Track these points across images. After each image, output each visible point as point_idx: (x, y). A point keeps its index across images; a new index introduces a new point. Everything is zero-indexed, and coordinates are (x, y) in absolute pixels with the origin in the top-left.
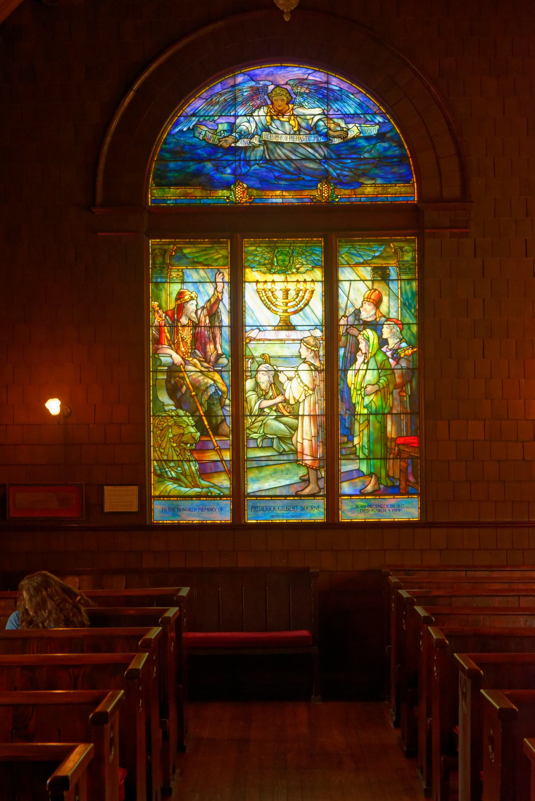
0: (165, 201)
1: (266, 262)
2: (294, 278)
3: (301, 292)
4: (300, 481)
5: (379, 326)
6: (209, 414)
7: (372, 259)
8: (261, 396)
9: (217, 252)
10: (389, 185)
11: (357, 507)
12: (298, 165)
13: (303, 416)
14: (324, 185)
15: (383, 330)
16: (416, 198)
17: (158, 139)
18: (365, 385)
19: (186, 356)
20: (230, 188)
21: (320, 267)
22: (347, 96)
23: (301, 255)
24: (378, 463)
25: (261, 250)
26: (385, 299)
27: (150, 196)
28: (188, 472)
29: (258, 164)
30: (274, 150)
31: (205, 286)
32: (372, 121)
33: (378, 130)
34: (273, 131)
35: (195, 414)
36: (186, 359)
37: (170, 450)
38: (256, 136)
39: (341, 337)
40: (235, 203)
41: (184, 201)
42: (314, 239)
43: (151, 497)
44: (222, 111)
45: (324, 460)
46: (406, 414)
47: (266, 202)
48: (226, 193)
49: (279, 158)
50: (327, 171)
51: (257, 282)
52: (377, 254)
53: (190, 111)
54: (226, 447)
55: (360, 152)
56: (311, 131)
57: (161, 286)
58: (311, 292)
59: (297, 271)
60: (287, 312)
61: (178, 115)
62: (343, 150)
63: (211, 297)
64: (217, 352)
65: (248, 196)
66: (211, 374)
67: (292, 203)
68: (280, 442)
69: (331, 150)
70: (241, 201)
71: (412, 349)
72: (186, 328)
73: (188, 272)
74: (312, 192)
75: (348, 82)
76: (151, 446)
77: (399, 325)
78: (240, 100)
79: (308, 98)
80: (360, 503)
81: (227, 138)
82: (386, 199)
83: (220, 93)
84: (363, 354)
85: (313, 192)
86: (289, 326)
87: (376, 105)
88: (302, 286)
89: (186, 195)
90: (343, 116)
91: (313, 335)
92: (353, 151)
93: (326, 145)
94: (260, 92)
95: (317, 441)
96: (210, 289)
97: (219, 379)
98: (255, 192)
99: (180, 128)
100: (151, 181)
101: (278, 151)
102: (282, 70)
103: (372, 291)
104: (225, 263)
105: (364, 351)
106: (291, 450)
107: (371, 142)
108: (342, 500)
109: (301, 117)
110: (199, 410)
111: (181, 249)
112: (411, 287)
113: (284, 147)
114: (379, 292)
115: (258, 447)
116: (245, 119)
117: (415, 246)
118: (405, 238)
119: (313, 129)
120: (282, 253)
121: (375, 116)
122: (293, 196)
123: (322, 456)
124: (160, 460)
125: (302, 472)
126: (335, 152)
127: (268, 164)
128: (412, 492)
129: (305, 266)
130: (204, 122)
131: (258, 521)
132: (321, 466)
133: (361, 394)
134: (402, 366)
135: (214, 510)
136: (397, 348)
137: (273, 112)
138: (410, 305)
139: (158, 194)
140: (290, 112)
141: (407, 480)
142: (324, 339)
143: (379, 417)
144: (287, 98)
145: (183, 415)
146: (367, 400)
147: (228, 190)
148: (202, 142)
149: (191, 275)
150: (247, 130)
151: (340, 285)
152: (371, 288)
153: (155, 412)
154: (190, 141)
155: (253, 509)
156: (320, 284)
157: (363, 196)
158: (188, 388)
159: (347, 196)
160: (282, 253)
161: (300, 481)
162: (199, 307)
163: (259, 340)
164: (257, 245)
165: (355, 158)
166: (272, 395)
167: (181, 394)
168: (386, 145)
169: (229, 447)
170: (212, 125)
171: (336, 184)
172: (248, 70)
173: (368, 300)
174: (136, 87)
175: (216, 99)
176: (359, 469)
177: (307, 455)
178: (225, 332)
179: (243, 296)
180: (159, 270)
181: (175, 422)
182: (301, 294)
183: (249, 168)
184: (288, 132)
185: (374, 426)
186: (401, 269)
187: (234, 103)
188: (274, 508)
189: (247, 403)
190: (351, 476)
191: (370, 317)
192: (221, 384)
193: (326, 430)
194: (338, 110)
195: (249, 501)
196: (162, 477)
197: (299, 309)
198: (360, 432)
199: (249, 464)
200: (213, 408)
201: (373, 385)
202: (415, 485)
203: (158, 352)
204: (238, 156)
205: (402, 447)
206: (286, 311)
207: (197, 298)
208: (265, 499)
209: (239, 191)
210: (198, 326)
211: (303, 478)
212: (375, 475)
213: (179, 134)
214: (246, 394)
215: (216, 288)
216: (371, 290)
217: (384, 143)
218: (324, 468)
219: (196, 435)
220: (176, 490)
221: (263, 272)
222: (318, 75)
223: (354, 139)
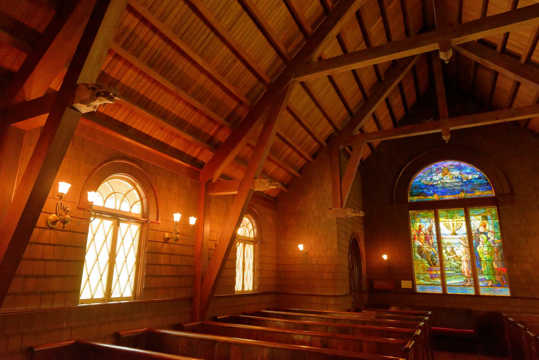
0: (413, 200)
1: (446, 216)
6: (432, 260)
11: (486, 290)
13: (463, 261)
22: (467, 168)
24: (492, 276)
26: (487, 225)
28: (427, 277)
41: (419, 200)
43: (415, 284)
46: (500, 261)
48: (431, 197)
50: (463, 189)
51: (444, 221)
52: (483, 212)
57: (414, 223)
66: (431, 248)
71: (499, 240)
78: (433, 172)
80: (487, 289)
86: (455, 234)
89: (419, 198)
93: (462, 182)
96: (429, 224)
98: (440, 196)
101: (446, 185)
105: (482, 241)
106: (460, 271)
112: (496, 221)
116: (435, 177)
119: (457, 178)
125: (465, 278)
128: (505, 286)
141: (504, 282)
143: (490, 262)
146: (485, 256)
154: (419, 184)
156: (464, 221)
158: (424, 252)
163: (446, 238)
168: (482, 180)
171: (466, 192)
174: (402, 171)
179: (439, 226)
182: (458, 224)
185: (488, 264)
190: (482, 280)
199: (446, 275)
205: (500, 271)
206: (454, 230)
215: (431, 224)
222: (457, 163)
223: (470, 179)
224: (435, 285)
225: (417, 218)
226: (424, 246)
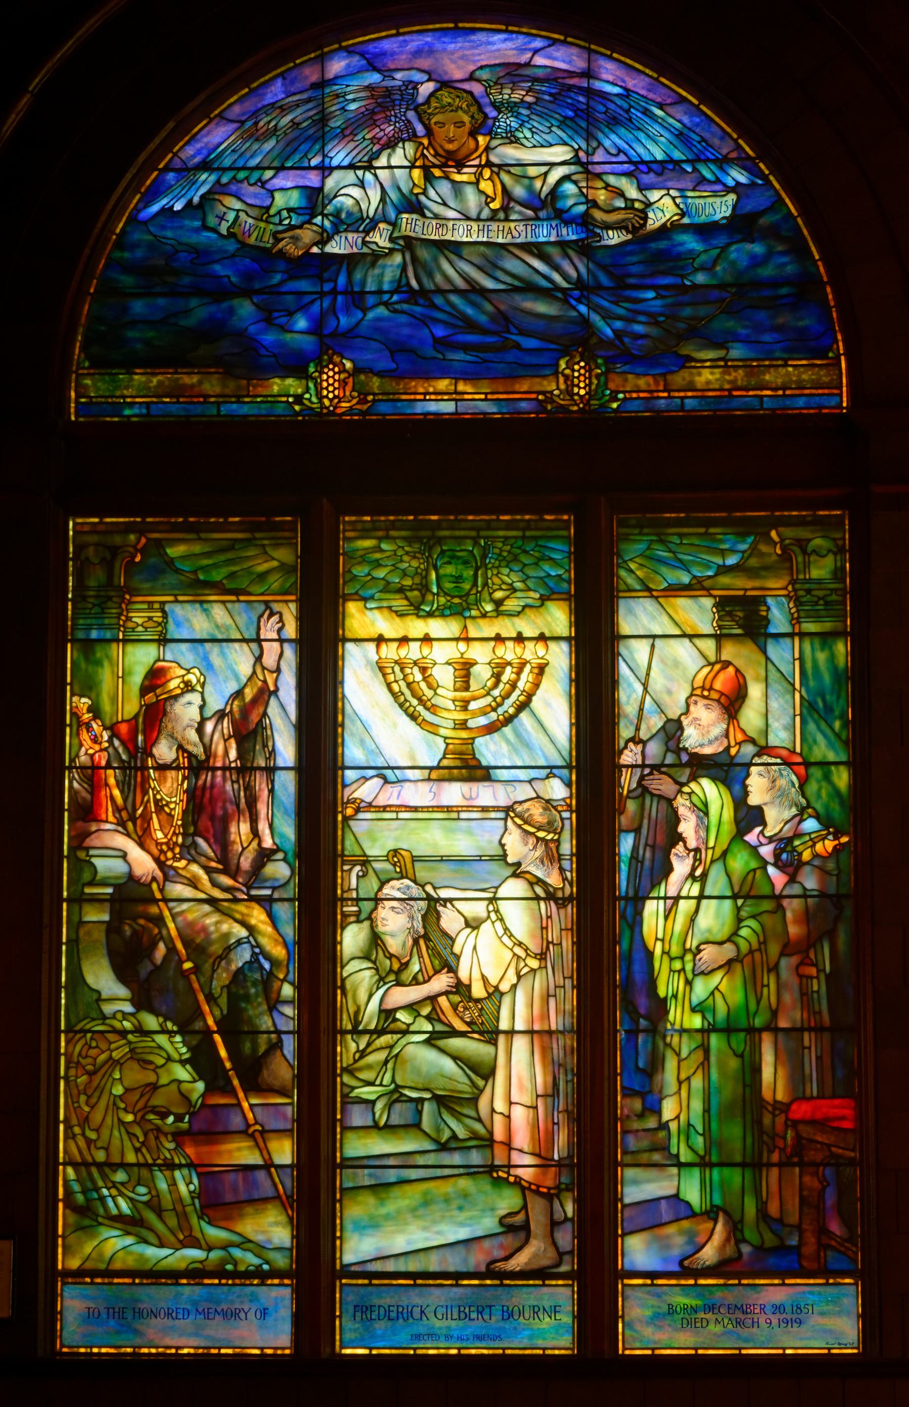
0: (117, 409)
1: (408, 582)
2: (488, 629)
3: (508, 669)
4: (500, 1230)
5: (738, 768)
7: (716, 575)
8: (388, 974)
9: (266, 553)
10: (767, 363)
11: (672, 1310)
12: (502, 307)
13: (511, 1033)
14: (578, 363)
15: (748, 782)
16: (845, 399)
17: (97, 230)
18: (695, 944)
19: (170, 855)
20: (307, 370)
21: (565, 597)
22: (646, 112)
23: (509, 562)
24: (735, 1177)
25: (394, 547)
26: (755, 691)
27: (73, 394)
28: (167, 1201)
29: (386, 304)
30: (433, 265)
31: (226, 651)
32: (718, 181)
33: (735, 207)
34: (431, 212)
35: (190, 1028)
36: (169, 863)
37: (116, 1133)
38: (382, 226)
39: (623, 800)
40: (320, 414)
41: (170, 406)
42: (548, 517)
43: (53, 1274)
44: (285, 155)
45: (571, 1166)
46: (818, 1029)
47: (409, 411)
48: (293, 385)
49: (447, 287)
50: (585, 322)
51: (380, 640)
52: (731, 560)
53: (194, 156)
54: (281, 1125)
55: (683, 268)
56: (541, 209)
58: (536, 671)
59: (496, 610)
60: (467, 728)
61: (161, 166)
62: (633, 264)
63: (245, 685)
64: (259, 844)
65: (355, 394)
66: (241, 908)
67: (485, 414)
68: (443, 1110)
69: (594, 262)
70: (335, 408)
71: (836, 838)
72: (171, 774)
73: (178, 611)
74: (541, 384)
75: (647, 71)
76: (57, 1122)
77: (795, 768)
79: (533, 117)
80: (681, 1300)
81: (298, 232)
82: (756, 403)
83: (279, 104)
84: (690, 851)
85: (545, 383)
87: (727, 138)
88: (509, 652)
89: (177, 391)
90: (633, 168)
91: (541, 795)
92: (662, 267)
93: (585, 249)
94: (393, 101)
95: (551, 1110)
97: (263, 922)
98: (376, 382)
99: (164, 202)
100: (77, 351)
102: (460, 39)
103: (717, 667)
104: (288, 585)
105: (692, 844)
106: (475, 1136)
107: (715, 242)
108: (626, 1288)
109: (512, 170)
110: (202, 1015)
111: (160, 545)
112: (832, 658)
113: (461, 257)
114: (737, 671)
115: (376, 1126)
116: (350, 176)
117: (844, 538)
118: (814, 515)
120: (452, 557)
121: (725, 166)
122: (486, 394)
123: (565, 1154)
124: (86, 1164)
126: (610, 269)
127: (417, 304)
128: (837, 1266)
129: (519, 594)
130: (233, 188)
131: (374, 1352)
132: (563, 1186)
133: (683, 969)
134: (805, 889)
135: (242, 1315)
136: (791, 834)
137: (431, 158)
138: (829, 709)
139: (98, 389)
140: (480, 156)
141: (822, 1231)
142: (574, 808)
143: (739, 1040)
144: (472, 117)
145: (158, 1028)
146: (701, 989)
147: (299, 378)
148: (225, 242)
149: (188, 620)
150: (356, 209)
151: (622, 650)
152: (713, 659)
153: (73, 1020)
154: (194, 239)
155: (358, 1314)
156: (564, 646)
157: (690, 394)
158: (171, 949)
159: (642, 395)
160: (453, 558)
161: (500, 1230)
162: (208, 713)
163: (384, 808)
164: (380, 534)
165: (666, 287)
166: (421, 970)
167: (150, 967)
168: (758, 248)
169: (289, 1127)
170: (255, 196)
171: (609, 360)
172: (361, 39)
173: (706, 693)
175: (269, 122)
176: (676, 1196)
177: (521, 1151)
178: (284, 785)
180: (94, 605)
181: (132, 1051)
182: (508, 674)
183: (360, 315)
184: (474, 214)
186: (801, 604)
187: (320, 133)
188: (422, 1312)
189: (344, 993)
191: (710, 742)
192: (270, 937)
193: (578, 1075)
194: (620, 151)
195: (346, 1289)
196: (90, 1214)
197: (501, 717)
198: (680, 1083)
200: (245, 1010)
201: (721, 943)
202: (847, 1245)
203: (89, 842)
204: (329, 280)
205: (805, 1131)
206: (462, 725)
207: (203, 685)
208: (394, 1282)
209: (330, 378)
210: (203, 768)
211: (509, 1220)
212: (726, 1213)
213: (161, 220)
214: (342, 967)
215: (259, 659)
216: (712, 664)
217: (753, 242)
218: (573, 1191)
219: (192, 1090)
220: (130, 1253)
221: (396, 612)
223: (664, 231)
224: (235, 1274)
225: (134, 592)
226: (179, 890)
